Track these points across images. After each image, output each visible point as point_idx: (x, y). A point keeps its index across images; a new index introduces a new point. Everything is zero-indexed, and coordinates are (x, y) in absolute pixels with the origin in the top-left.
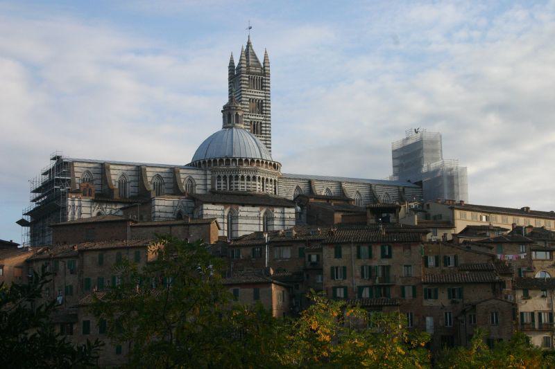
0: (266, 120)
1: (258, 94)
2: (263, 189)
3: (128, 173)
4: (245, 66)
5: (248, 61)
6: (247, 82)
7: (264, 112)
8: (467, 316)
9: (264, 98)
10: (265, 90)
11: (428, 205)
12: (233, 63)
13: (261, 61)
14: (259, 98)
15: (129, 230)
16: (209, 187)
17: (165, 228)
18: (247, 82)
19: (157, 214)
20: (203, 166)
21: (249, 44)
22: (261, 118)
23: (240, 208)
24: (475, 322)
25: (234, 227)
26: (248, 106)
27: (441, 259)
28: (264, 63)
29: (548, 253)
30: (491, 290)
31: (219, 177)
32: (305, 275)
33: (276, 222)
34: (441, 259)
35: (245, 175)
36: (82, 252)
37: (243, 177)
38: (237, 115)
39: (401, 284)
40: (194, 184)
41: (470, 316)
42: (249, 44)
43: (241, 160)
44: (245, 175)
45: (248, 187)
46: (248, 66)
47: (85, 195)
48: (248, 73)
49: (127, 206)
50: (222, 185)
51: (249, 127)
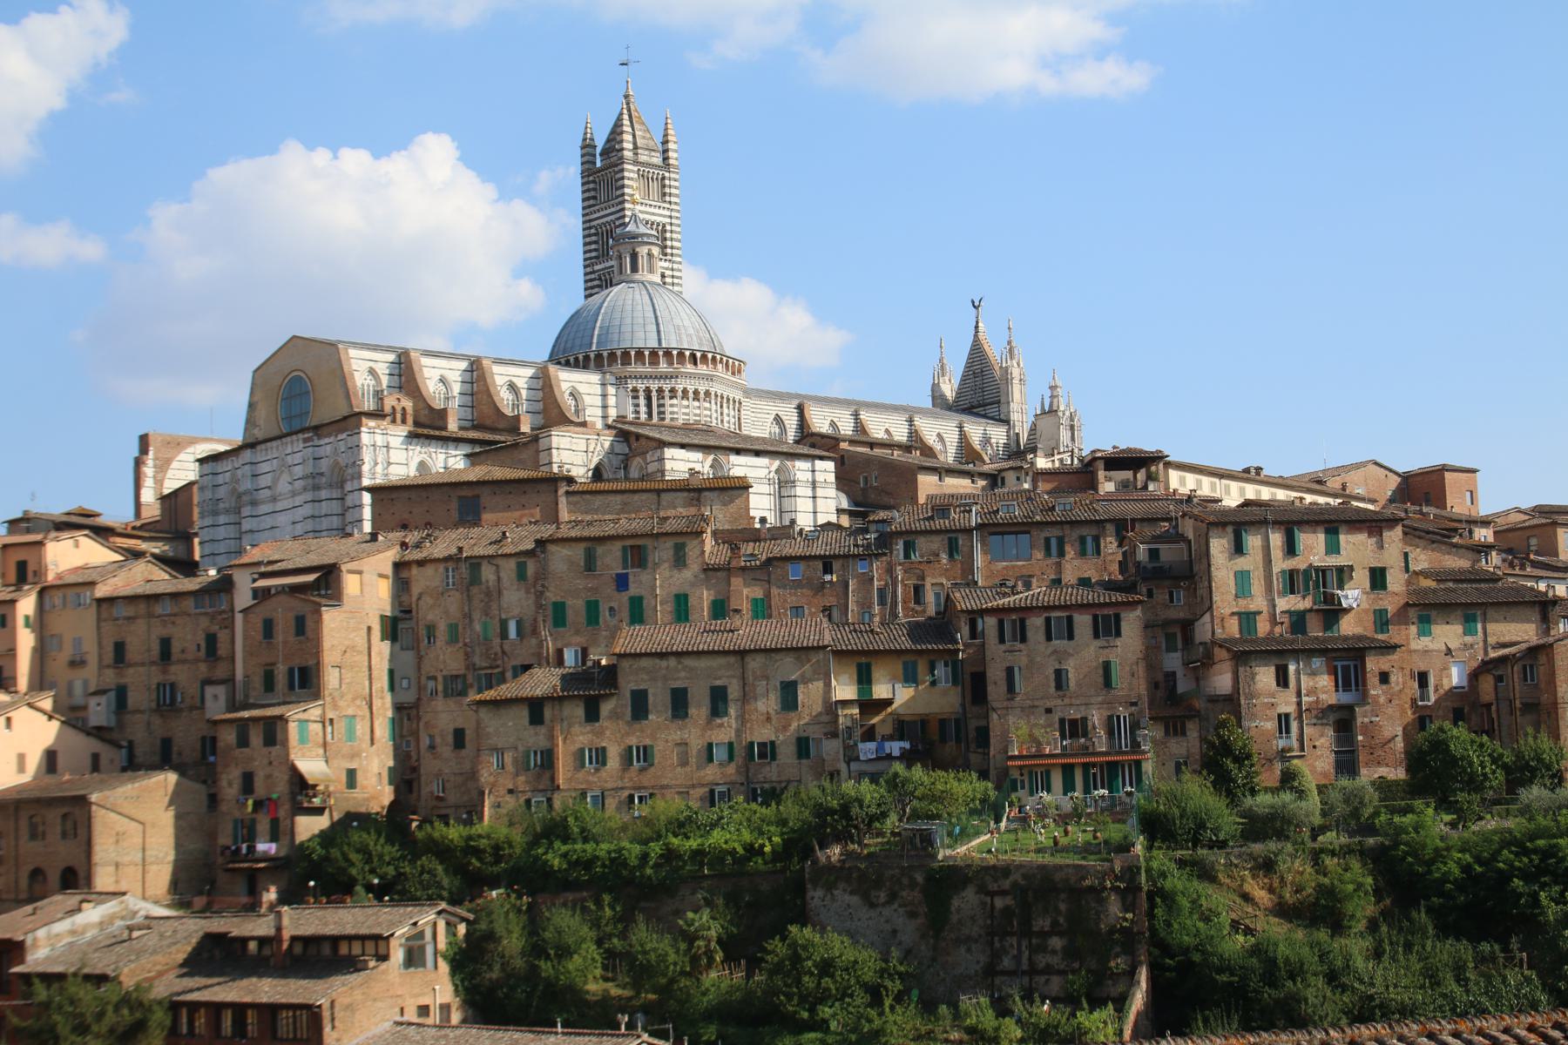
1: (656, 211)
4: (630, 146)
5: (634, 136)
10: (670, 203)
14: (658, 219)
15: (563, 501)
16: (613, 413)
17: (644, 496)
23: (734, 458)
24: (1532, 680)
31: (635, 390)
33: (799, 491)
35: (691, 389)
36: (541, 543)
37: (685, 391)
38: (650, 255)
43: (626, 354)
44: (691, 389)
46: (636, 147)
47: (394, 421)
48: (636, 163)
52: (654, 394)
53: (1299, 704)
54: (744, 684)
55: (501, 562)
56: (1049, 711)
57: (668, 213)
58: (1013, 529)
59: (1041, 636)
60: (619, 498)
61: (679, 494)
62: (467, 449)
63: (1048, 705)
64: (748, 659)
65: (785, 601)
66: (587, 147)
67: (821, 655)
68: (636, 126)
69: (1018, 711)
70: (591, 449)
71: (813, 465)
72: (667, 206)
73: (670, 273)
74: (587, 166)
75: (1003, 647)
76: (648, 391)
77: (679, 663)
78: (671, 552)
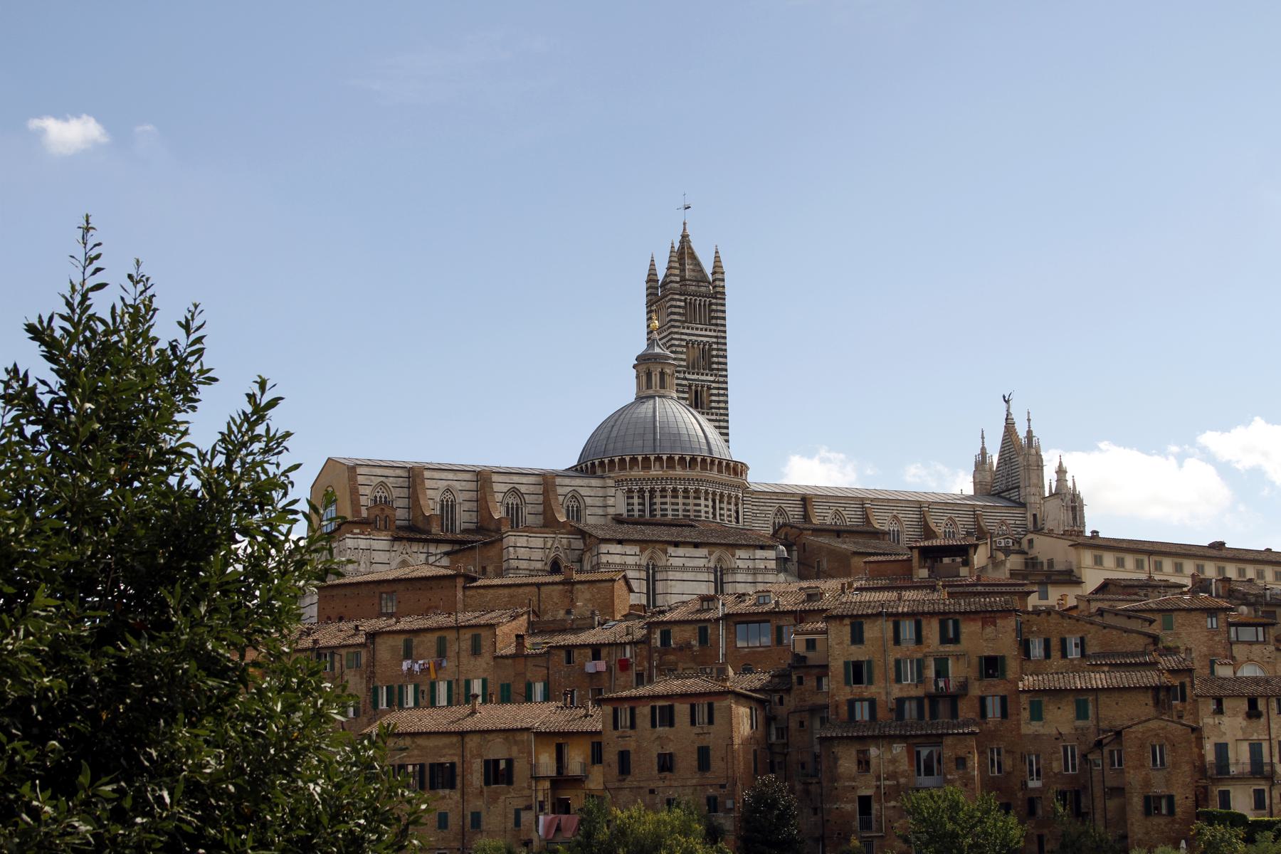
0: (718, 382)
1: (703, 333)
2: (714, 516)
3: (458, 485)
4: (678, 279)
5: (683, 270)
6: (681, 311)
7: (715, 366)
8: (1106, 750)
9: (714, 340)
10: (717, 325)
11: (1031, 541)
12: (656, 275)
13: (708, 269)
15: (460, 594)
17: (527, 589)
18: (681, 311)
19: (514, 563)
20: (599, 472)
21: (685, 237)
22: (712, 378)
23: (671, 550)
24: (1120, 764)
25: (660, 587)
26: (684, 356)
27: (1055, 643)
28: (714, 273)
29: (1260, 629)
30: (1151, 703)
31: (630, 491)
32: (794, 678)
34: (1055, 643)
36: (372, 636)
38: (662, 374)
39: (980, 694)
40: (582, 506)
41: (1111, 752)
42: (685, 237)
45: (685, 510)
49: (457, 547)
50: (636, 507)
51: (686, 396)
52: (647, 494)
53: (878, 787)
54: (463, 761)
55: (343, 652)
56: (652, 791)
57: (714, 334)
58: (755, 619)
59: (648, 724)
60: (506, 591)
61: (555, 587)
62: (446, 548)
63: (652, 786)
64: (467, 739)
65: (560, 685)
66: (652, 279)
67: (525, 736)
68: (687, 261)
69: (627, 792)
70: (549, 545)
71: (754, 555)
72: (713, 327)
73: (714, 385)
74: (649, 298)
75: (616, 733)
76: (641, 491)
77: (413, 742)
78: (469, 642)
